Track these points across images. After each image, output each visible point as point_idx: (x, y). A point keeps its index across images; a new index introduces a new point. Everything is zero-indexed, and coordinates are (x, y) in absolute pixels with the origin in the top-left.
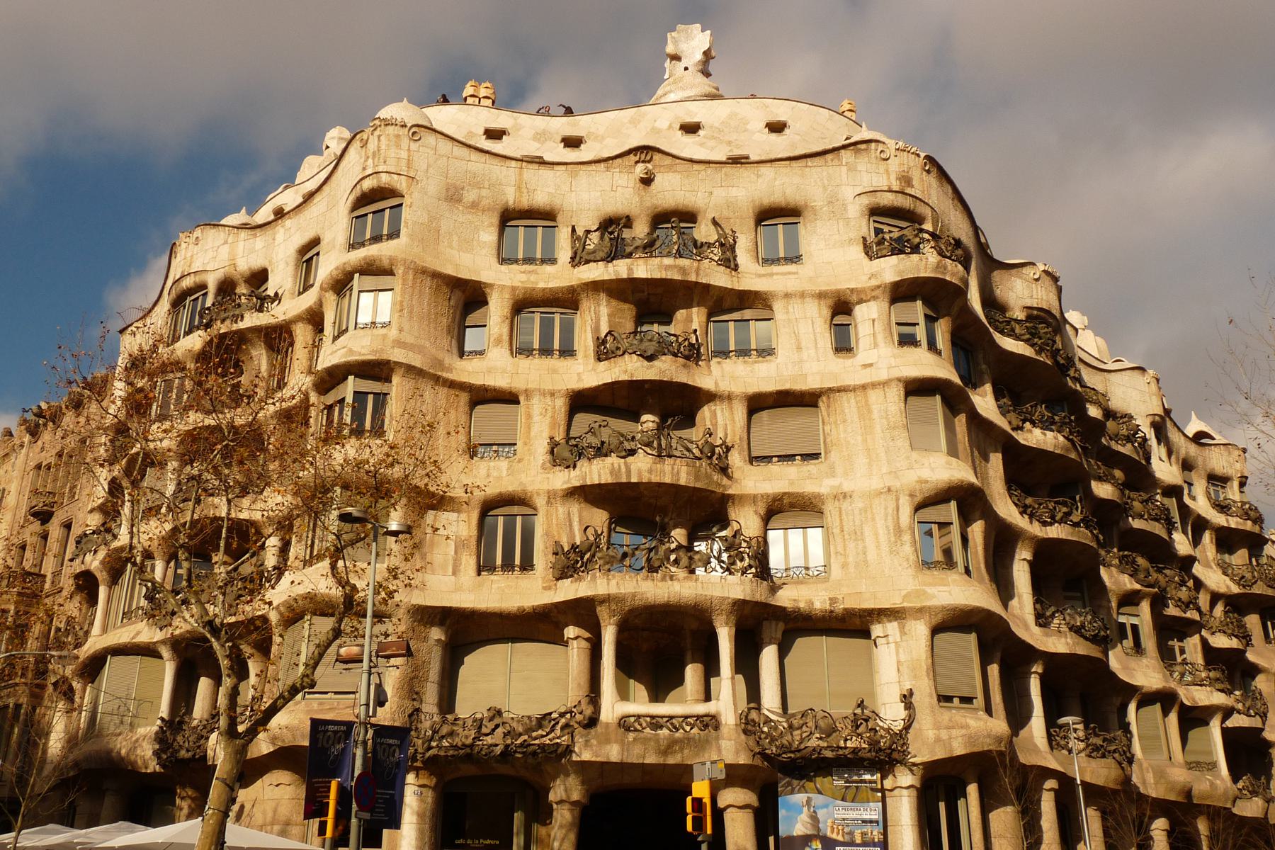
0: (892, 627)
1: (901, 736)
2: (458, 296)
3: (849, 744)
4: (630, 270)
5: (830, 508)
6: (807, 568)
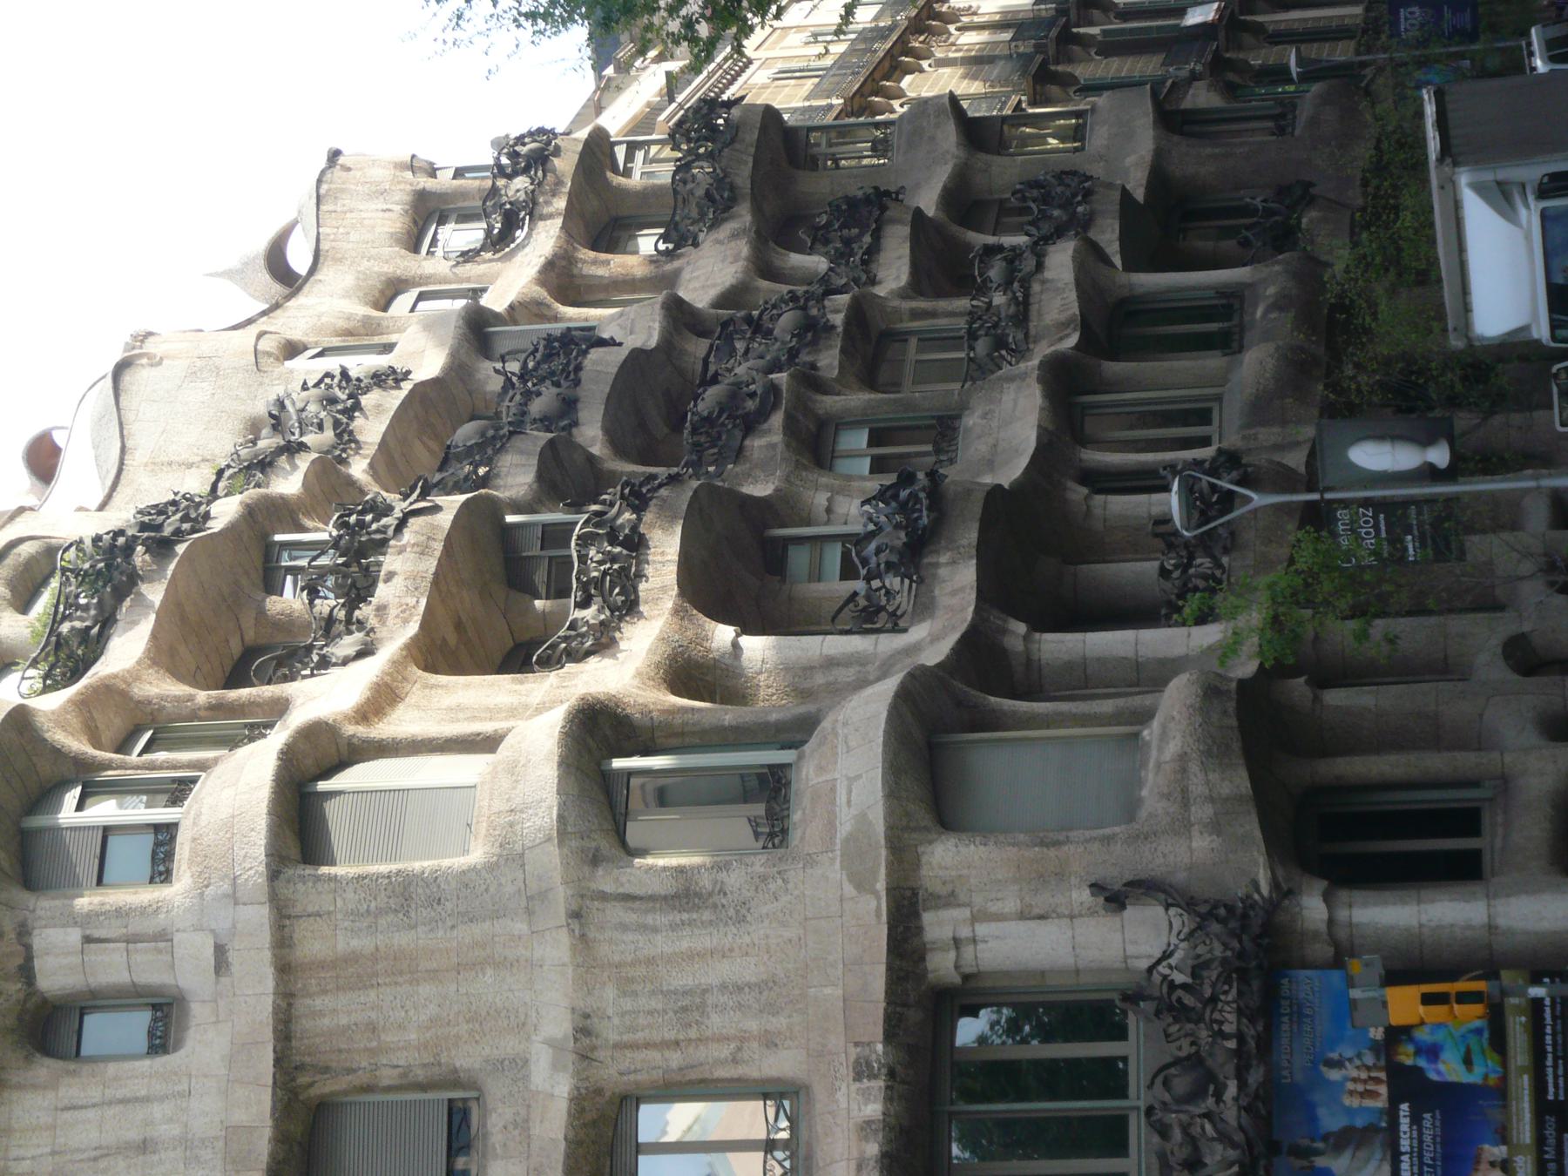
0: (937, 925)
1: (1204, 910)
3: (1227, 1028)
5: (613, 1072)
6: (769, 1146)
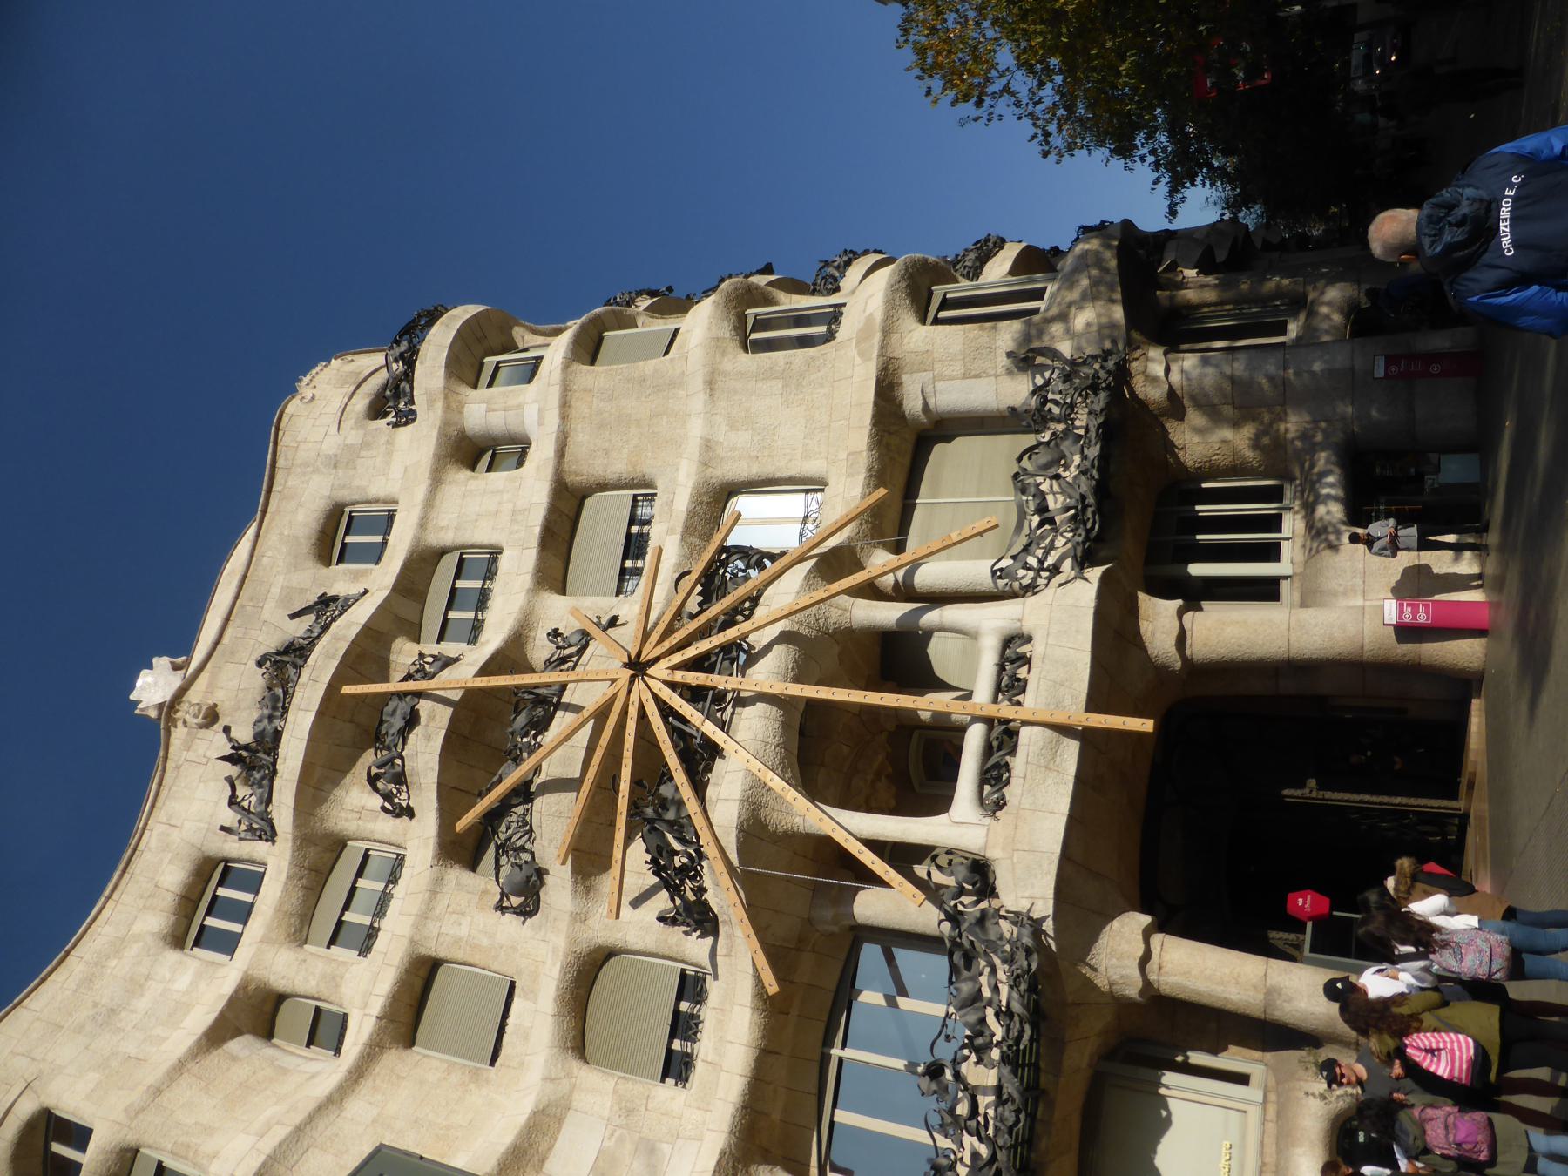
2: (243, 1046)
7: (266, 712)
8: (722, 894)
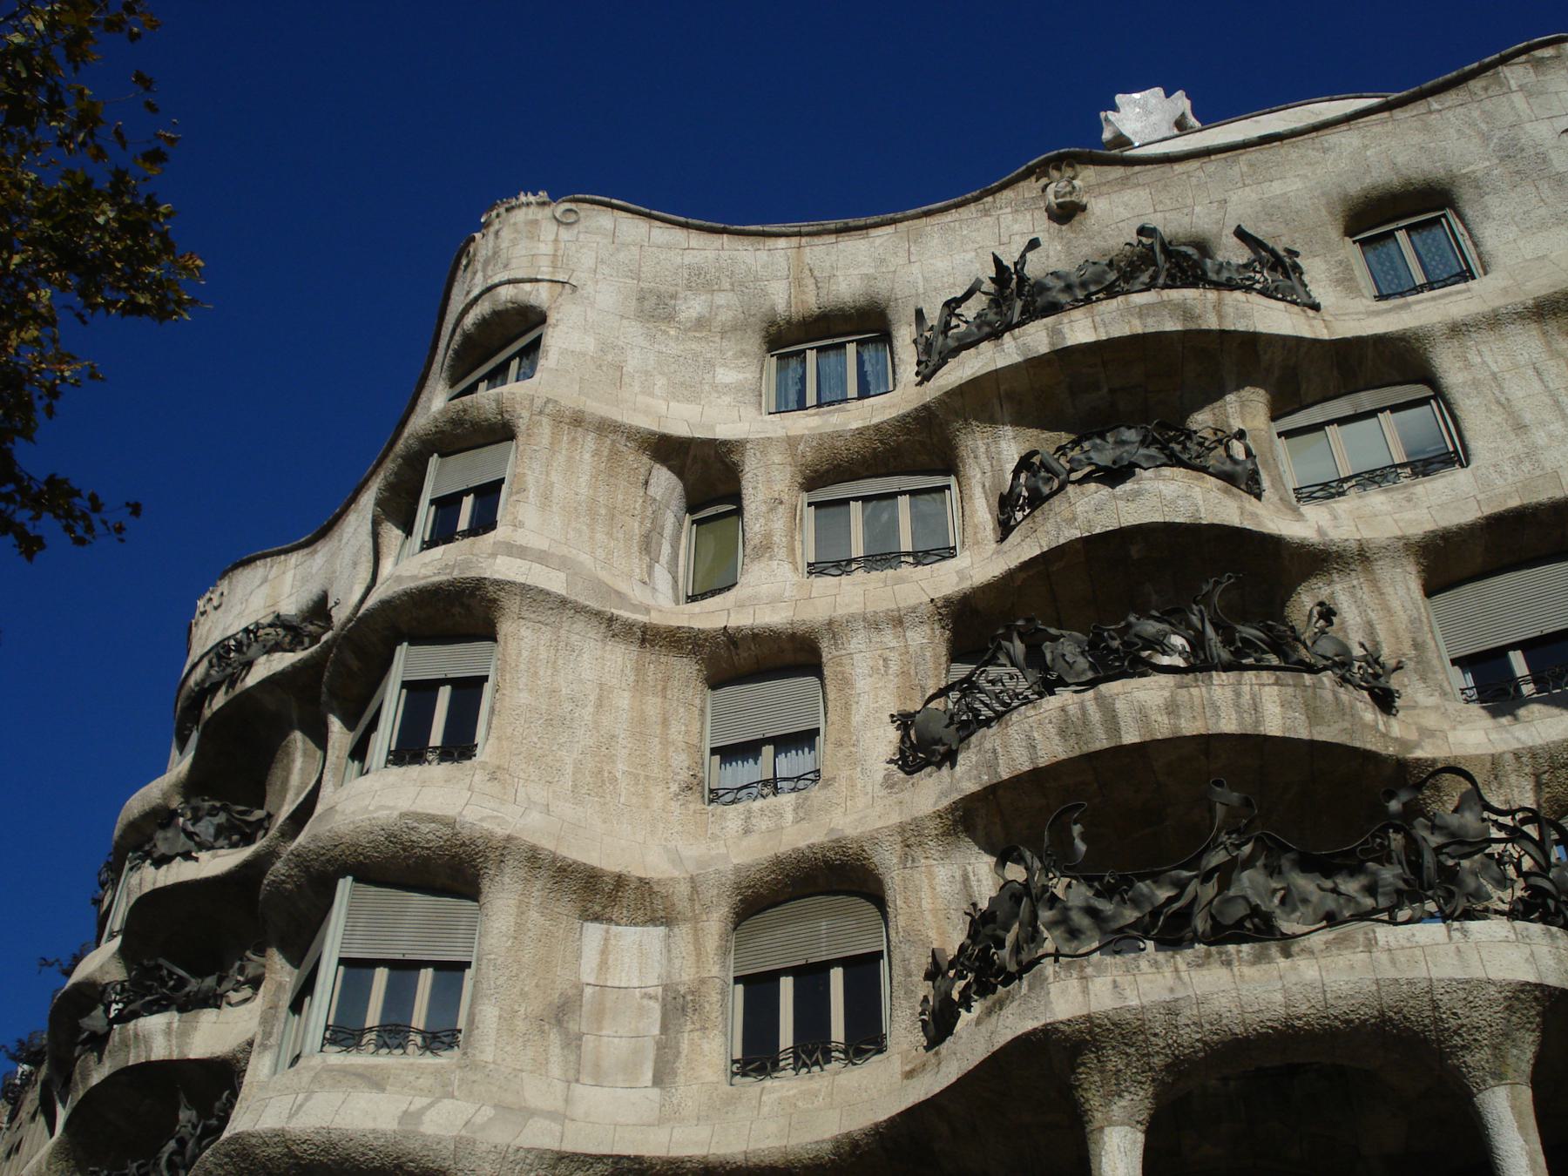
4: (1055, 332)
7: (1074, 279)
8: (980, 1035)
